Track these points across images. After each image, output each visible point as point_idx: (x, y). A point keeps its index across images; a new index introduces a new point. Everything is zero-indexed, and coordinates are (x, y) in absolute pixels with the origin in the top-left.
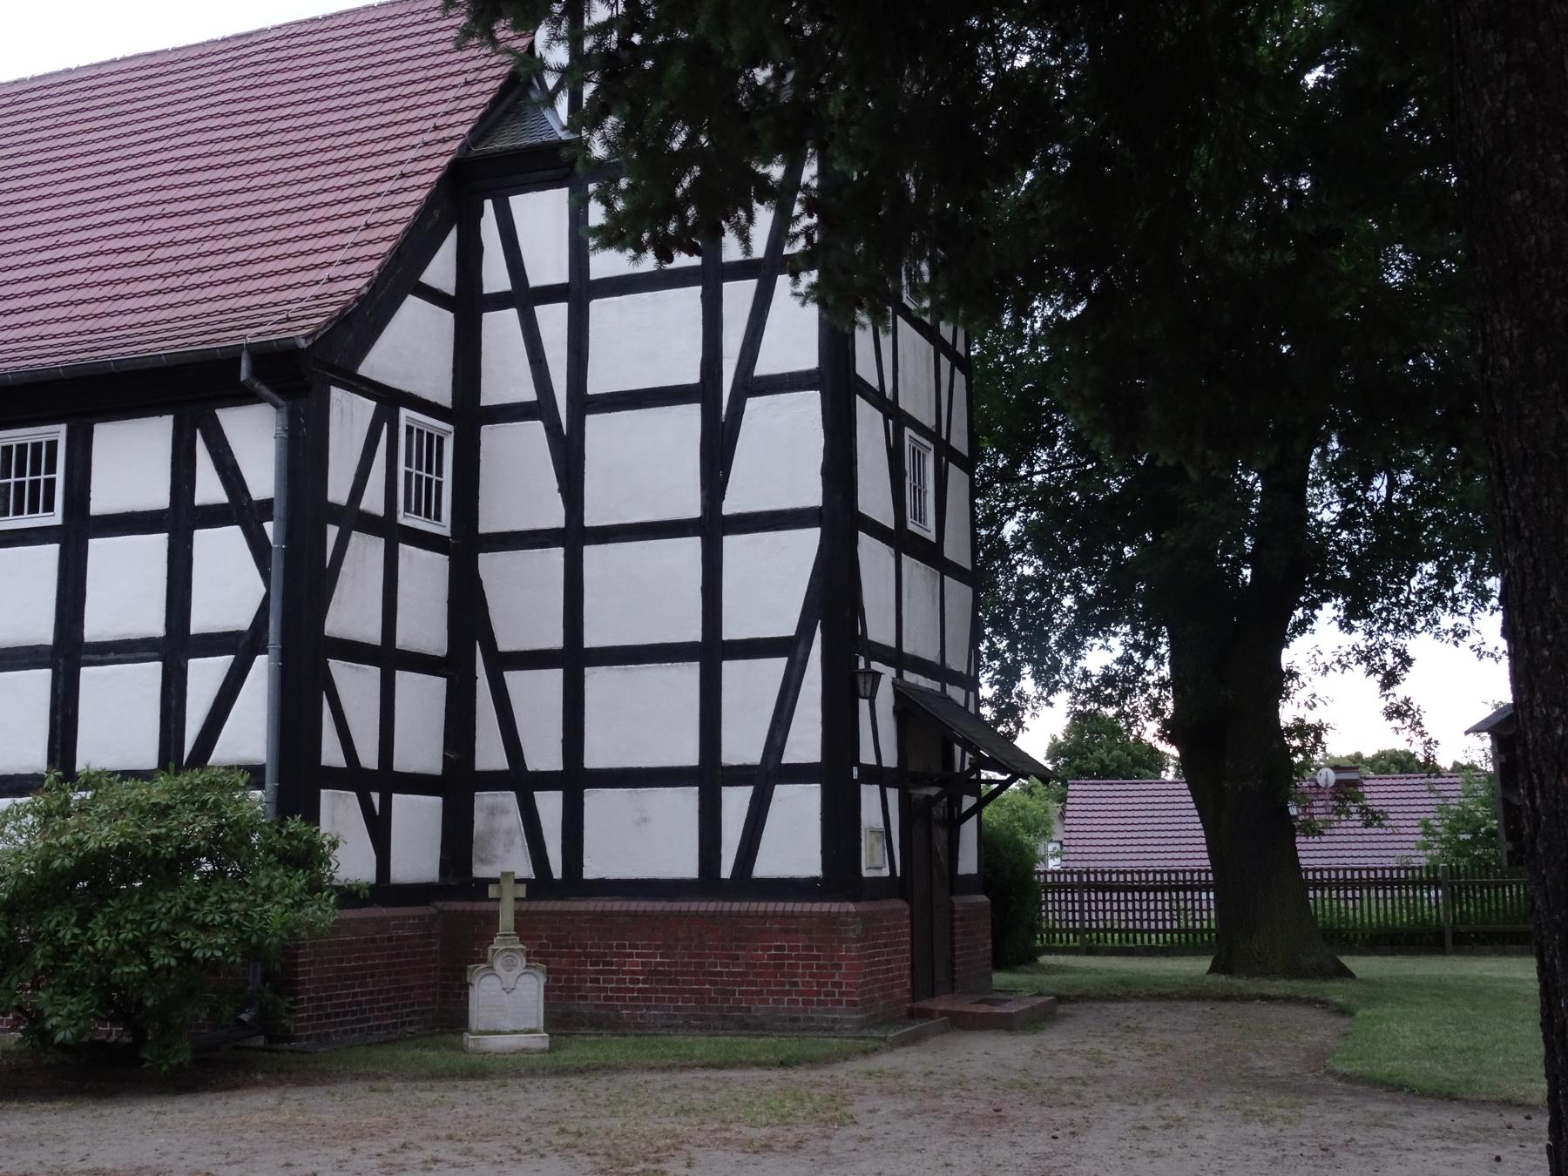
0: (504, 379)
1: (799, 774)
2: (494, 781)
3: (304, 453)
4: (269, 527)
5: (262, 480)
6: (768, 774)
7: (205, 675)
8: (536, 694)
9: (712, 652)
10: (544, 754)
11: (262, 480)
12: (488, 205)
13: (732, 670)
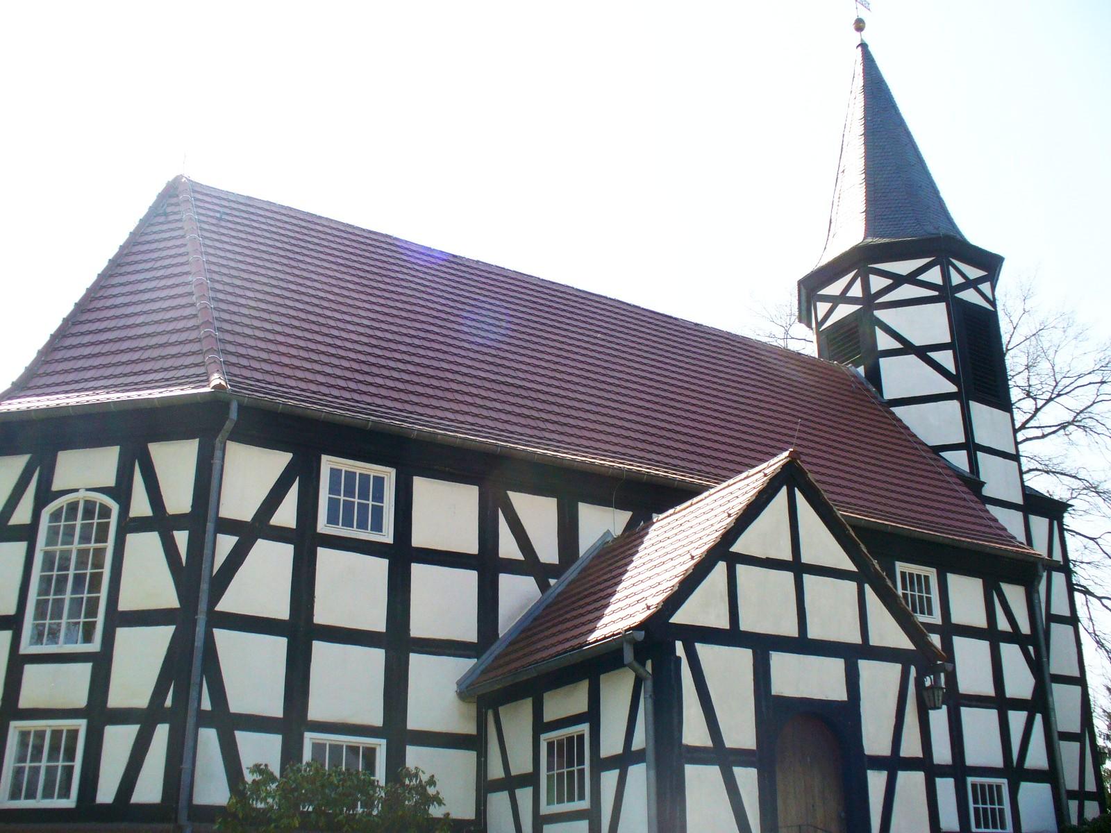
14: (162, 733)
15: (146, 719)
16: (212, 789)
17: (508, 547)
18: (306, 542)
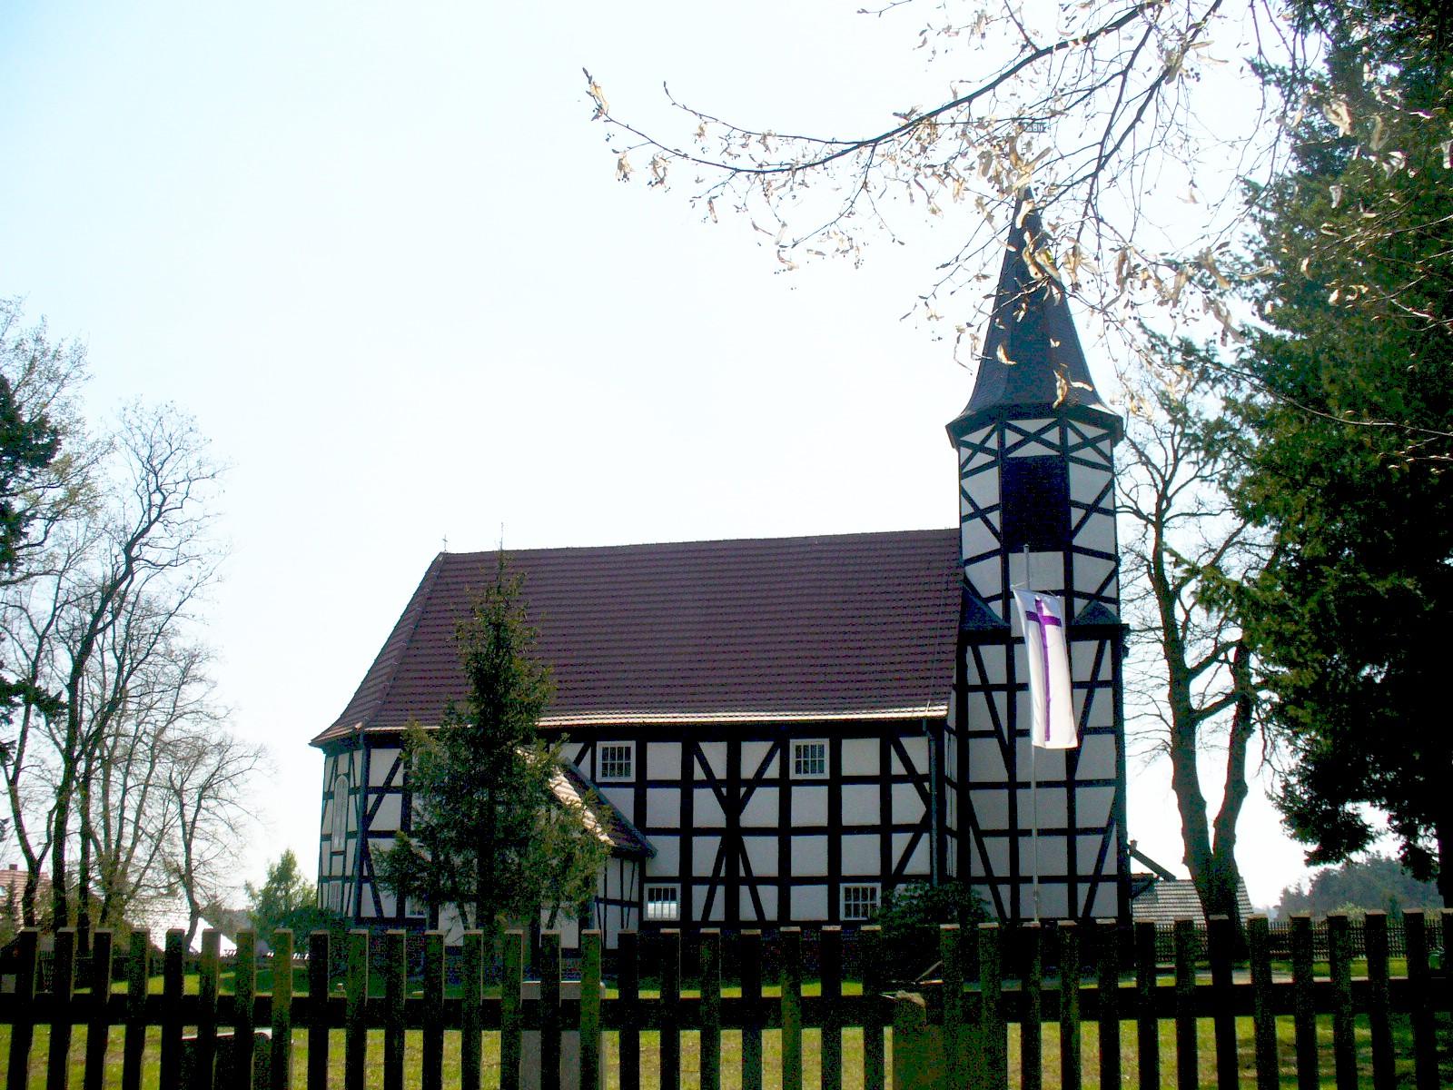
0: (979, 718)
1: (1109, 878)
2: (979, 881)
3: (938, 758)
4: (927, 785)
5: (922, 766)
6: (1096, 878)
7: (900, 842)
8: (998, 849)
9: (1071, 832)
10: (1001, 868)
11: (922, 766)
12: (969, 648)
13: (1080, 839)
14: (720, 890)
15: (712, 882)
16: (747, 912)
17: (897, 768)
18: (785, 785)
